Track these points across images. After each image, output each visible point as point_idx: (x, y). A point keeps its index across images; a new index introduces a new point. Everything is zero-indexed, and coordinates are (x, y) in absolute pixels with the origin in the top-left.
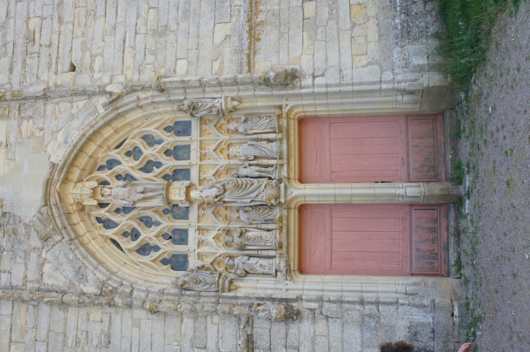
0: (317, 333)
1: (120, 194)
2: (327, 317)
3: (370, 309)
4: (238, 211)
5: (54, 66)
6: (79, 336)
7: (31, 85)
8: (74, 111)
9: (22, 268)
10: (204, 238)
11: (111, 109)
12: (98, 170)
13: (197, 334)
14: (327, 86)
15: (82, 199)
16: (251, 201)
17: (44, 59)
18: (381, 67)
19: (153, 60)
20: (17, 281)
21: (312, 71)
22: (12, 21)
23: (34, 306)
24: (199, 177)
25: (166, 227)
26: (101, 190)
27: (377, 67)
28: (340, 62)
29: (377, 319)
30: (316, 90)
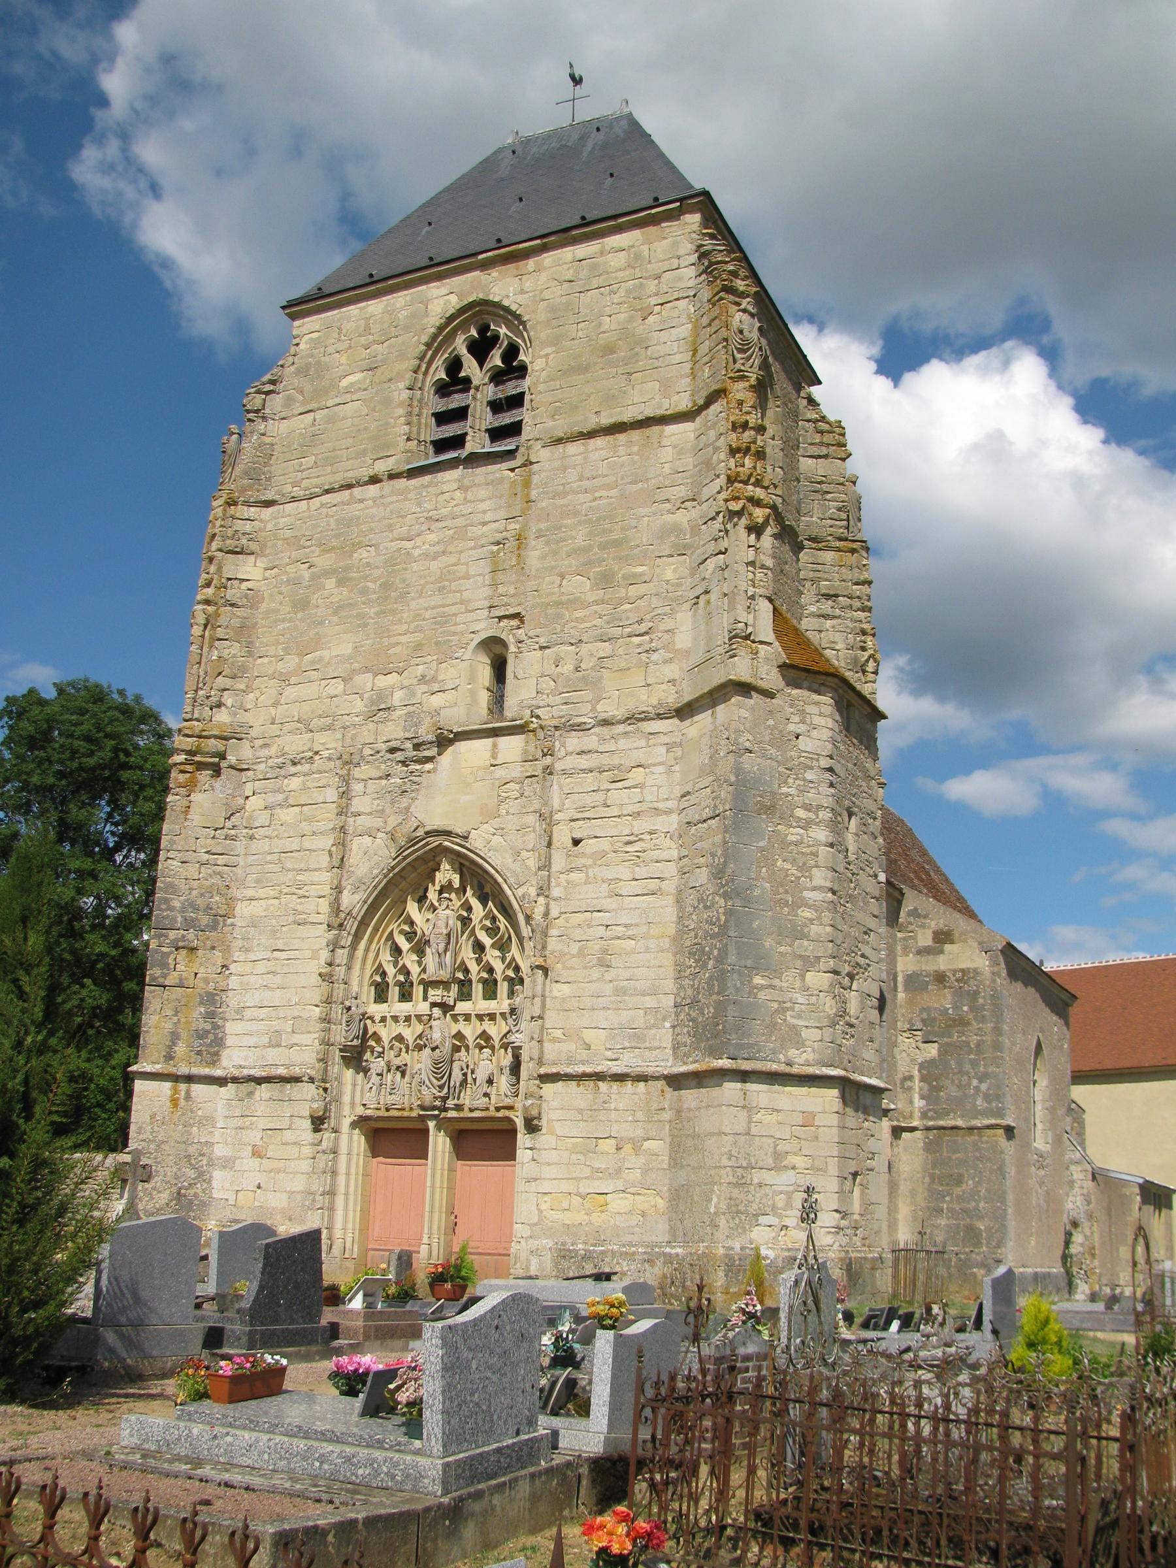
5: (580, 816)
8: (524, 854)
17: (589, 800)
18: (536, 1224)
22: (643, 743)
27: (535, 1220)
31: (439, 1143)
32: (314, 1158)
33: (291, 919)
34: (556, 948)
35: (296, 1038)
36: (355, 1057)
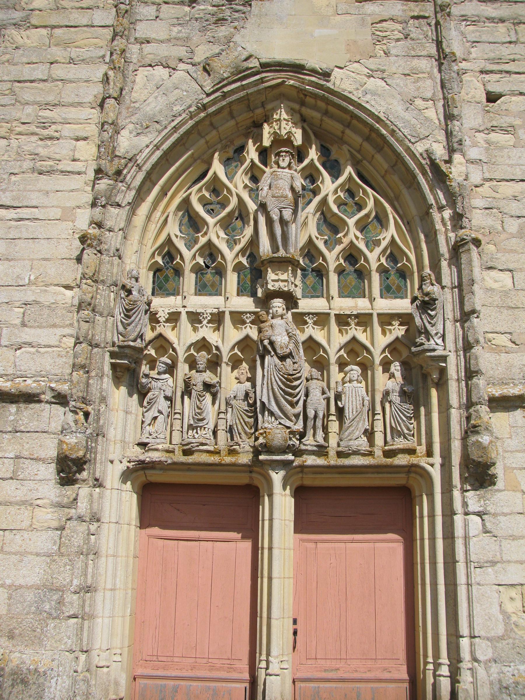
0: (37, 509)
1: (280, 181)
2: (62, 528)
3: (71, 603)
4: (248, 379)
5: (495, 67)
6: (54, 127)
7: (462, 33)
8: (419, 102)
9: (163, 35)
10: (205, 322)
11: (424, 162)
12: (322, 145)
13: (46, 311)
14: (466, 538)
15: (272, 123)
16: (263, 404)
18: (502, 638)
19: (510, 231)
20: (142, 30)
21: (492, 511)
23: (103, 57)
24: (309, 314)
25: (225, 260)
26: (287, 152)
27: (500, 630)
28: (509, 562)
29: (55, 615)
30: (458, 519)
31: (281, 506)
32: (62, 528)
33: (27, 165)
34: (484, 224)
35: (27, 335)
36: (129, 369)
